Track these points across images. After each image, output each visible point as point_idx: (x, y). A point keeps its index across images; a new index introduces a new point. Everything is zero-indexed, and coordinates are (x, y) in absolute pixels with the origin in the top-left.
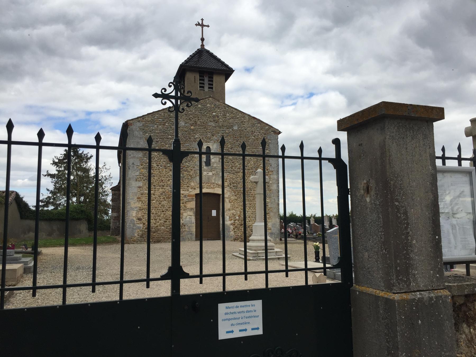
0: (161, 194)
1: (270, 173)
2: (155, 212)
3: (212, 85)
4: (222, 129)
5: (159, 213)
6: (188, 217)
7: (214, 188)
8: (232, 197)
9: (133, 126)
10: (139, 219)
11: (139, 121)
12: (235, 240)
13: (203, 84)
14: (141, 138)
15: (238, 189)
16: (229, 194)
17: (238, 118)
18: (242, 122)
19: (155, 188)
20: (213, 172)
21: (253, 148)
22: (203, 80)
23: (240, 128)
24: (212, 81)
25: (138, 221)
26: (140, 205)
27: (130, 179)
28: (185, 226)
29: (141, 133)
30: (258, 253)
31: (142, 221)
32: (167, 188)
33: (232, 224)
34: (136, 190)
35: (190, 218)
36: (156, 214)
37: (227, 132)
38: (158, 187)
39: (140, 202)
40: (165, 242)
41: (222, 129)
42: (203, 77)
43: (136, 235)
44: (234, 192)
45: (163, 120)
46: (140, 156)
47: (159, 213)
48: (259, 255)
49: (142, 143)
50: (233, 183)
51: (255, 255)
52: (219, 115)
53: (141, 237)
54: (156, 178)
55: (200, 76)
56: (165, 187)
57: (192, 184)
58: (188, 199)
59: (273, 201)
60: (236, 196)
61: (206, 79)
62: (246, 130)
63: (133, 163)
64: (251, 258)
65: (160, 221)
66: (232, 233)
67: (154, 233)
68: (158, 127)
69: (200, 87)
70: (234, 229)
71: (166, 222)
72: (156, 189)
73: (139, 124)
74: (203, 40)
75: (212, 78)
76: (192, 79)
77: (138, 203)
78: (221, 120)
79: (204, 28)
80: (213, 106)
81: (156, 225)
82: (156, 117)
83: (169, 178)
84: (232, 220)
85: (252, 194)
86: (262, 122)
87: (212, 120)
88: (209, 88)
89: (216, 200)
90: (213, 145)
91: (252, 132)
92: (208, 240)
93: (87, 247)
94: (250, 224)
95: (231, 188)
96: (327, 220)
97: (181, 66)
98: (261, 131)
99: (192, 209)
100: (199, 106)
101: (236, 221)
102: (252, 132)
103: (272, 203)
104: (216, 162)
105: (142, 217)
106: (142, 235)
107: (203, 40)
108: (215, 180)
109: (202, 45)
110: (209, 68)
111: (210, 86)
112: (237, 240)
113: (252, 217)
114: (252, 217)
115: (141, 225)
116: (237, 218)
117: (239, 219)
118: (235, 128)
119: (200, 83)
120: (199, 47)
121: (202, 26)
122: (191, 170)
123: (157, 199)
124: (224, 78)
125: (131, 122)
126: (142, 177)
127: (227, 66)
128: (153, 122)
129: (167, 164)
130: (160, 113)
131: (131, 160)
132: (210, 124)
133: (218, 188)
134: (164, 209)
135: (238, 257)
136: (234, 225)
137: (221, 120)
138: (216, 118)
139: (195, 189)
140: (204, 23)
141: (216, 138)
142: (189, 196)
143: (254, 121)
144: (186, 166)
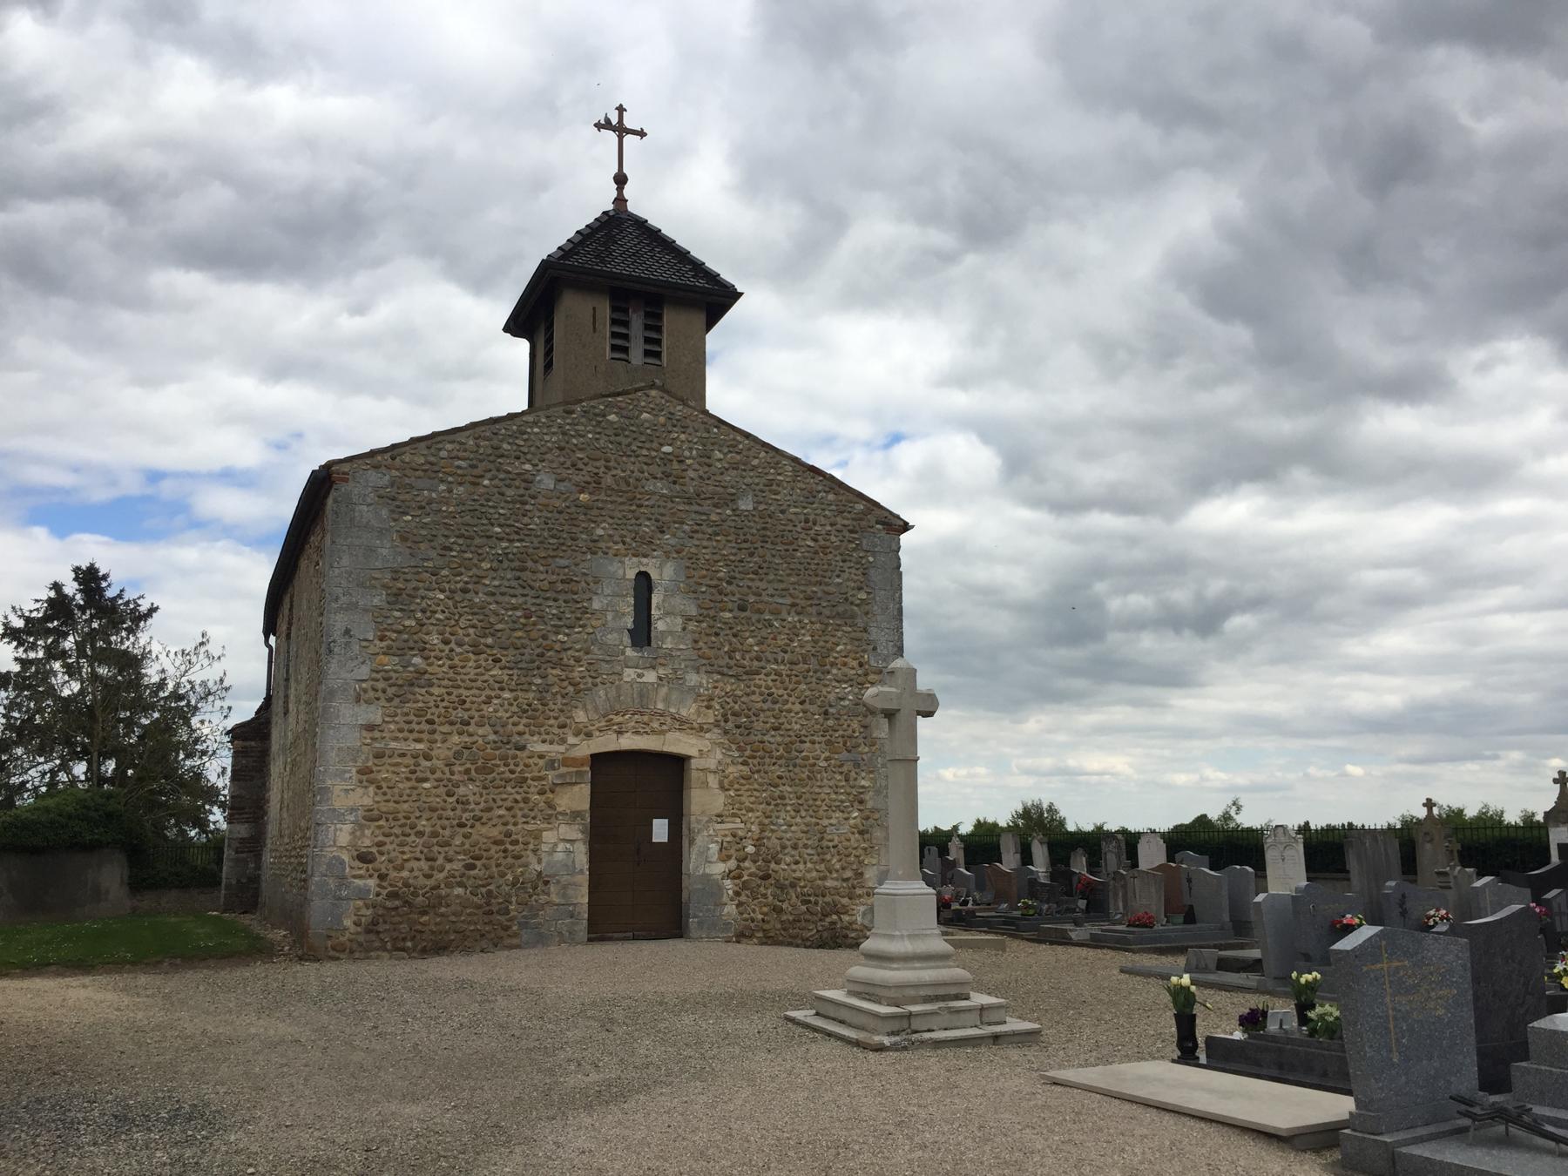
0: (457, 755)
1: (871, 677)
2: (428, 830)
3: (658, 342)
4: (696, 508)
5: (447, 833)
6: (561, 847)
7: (663, 733)
8: (731, 769)
9: (351, 484)
10: (364, 858)
11: (376, 467)
12: (741, 936)
13: (626, 337)
14: (381, 533)
15: (752, 737)
16: (719, 756)
17: (754, 468)
18: (770, 483)
19: (433, 732)
20: (661, 671)
21: (810, 583)
22: (626, 324)
23: (761, 507)
24: (659, 329)
25: (357, 864)
26: (367, 801)
27: (332, 694)
28: (546, 883)
29: (384, 513)
30: (910, 1015)
31: (376, 865)
32: (481, 731)
33: (728, 875)
34: (353, 739)
35: (568, 852)
36: (435, 834)
37: (714, 517)
38: (446, 728)
39: (372, 789)
40: (467, 951)
41: (696, 508)
42: (626, 311)
43: (348, 923)
44: (740, 749)
45: (473, 467)
46: (376, 601)
47: (447, 833)
48: (916, 1024)
49: (385, 552)
50: (735, 714)
51: (896, 1026)
52: (687, 453)
53: (368, 931)
55: (614, 309)
56: (471, 729)
57: (580, 716)
58: (561, 776)
60: (745, 763)
61: (637, 322)
62: (783, 512)
63: (347, 632)
64: (887, 1041)
65: (448, 866)
66: (730, 909)
67: (425, 913)
68: (450, 491)
69: (614, 348)
70: (737, 894)
71: (473, 867)
72: (437, 736)
73: (374, 477)
74: (621, 180)
75: (659, 317)
76: (580, 313)
77: (360, 791)
78: (691, 474)
79: (628, 139)
80: (662, 420)
82: (443, 454)
83: (488, 692)
84: (729, 857)
85: (806, 758)
86: (841, 484)
87: (658, 471)
88: (647, 353)
89: (663, 777)
90: (661, 567)
91: (807, 521)
93: (143, 979)
94: (798, 874)
95: (726, 732)
96: (1012, 850)
97: (546, 267)
98: (839, 519)
99: (576, 815)
100: (612, 417)
101: (747, 864)
102: (807, 521)
104: (671, 633)
105: (374, 850)
106: (374, 923)
107: (621, 180)
109: (620, 201)
110: (647, 281)
111: (649, 347)
112: (750, 937)
113: (806, 846)
114: (806, 846)
116: (750, 849)
118: (746, 504)
119: (614, 335)
120: (610, 207)
121: (621, 130)
122: (578, 660)
123: (438, 775)
124: (700, 318)
125: (346, 468)
126: (381, 685)
127: (713, 277)
128: (432, 471)
129: (485, 636)
130: (461, 437)
131: (339, 617)
132: (650, 486)
134: (466, 815)
135: (815, 1029)
137: (691, 474)
138: (676, 465)
139: (589, 735)
140: (628, 123)
141: (673, 541)
142: (567, 762)
143: (812, 481)
144: (557, 647)
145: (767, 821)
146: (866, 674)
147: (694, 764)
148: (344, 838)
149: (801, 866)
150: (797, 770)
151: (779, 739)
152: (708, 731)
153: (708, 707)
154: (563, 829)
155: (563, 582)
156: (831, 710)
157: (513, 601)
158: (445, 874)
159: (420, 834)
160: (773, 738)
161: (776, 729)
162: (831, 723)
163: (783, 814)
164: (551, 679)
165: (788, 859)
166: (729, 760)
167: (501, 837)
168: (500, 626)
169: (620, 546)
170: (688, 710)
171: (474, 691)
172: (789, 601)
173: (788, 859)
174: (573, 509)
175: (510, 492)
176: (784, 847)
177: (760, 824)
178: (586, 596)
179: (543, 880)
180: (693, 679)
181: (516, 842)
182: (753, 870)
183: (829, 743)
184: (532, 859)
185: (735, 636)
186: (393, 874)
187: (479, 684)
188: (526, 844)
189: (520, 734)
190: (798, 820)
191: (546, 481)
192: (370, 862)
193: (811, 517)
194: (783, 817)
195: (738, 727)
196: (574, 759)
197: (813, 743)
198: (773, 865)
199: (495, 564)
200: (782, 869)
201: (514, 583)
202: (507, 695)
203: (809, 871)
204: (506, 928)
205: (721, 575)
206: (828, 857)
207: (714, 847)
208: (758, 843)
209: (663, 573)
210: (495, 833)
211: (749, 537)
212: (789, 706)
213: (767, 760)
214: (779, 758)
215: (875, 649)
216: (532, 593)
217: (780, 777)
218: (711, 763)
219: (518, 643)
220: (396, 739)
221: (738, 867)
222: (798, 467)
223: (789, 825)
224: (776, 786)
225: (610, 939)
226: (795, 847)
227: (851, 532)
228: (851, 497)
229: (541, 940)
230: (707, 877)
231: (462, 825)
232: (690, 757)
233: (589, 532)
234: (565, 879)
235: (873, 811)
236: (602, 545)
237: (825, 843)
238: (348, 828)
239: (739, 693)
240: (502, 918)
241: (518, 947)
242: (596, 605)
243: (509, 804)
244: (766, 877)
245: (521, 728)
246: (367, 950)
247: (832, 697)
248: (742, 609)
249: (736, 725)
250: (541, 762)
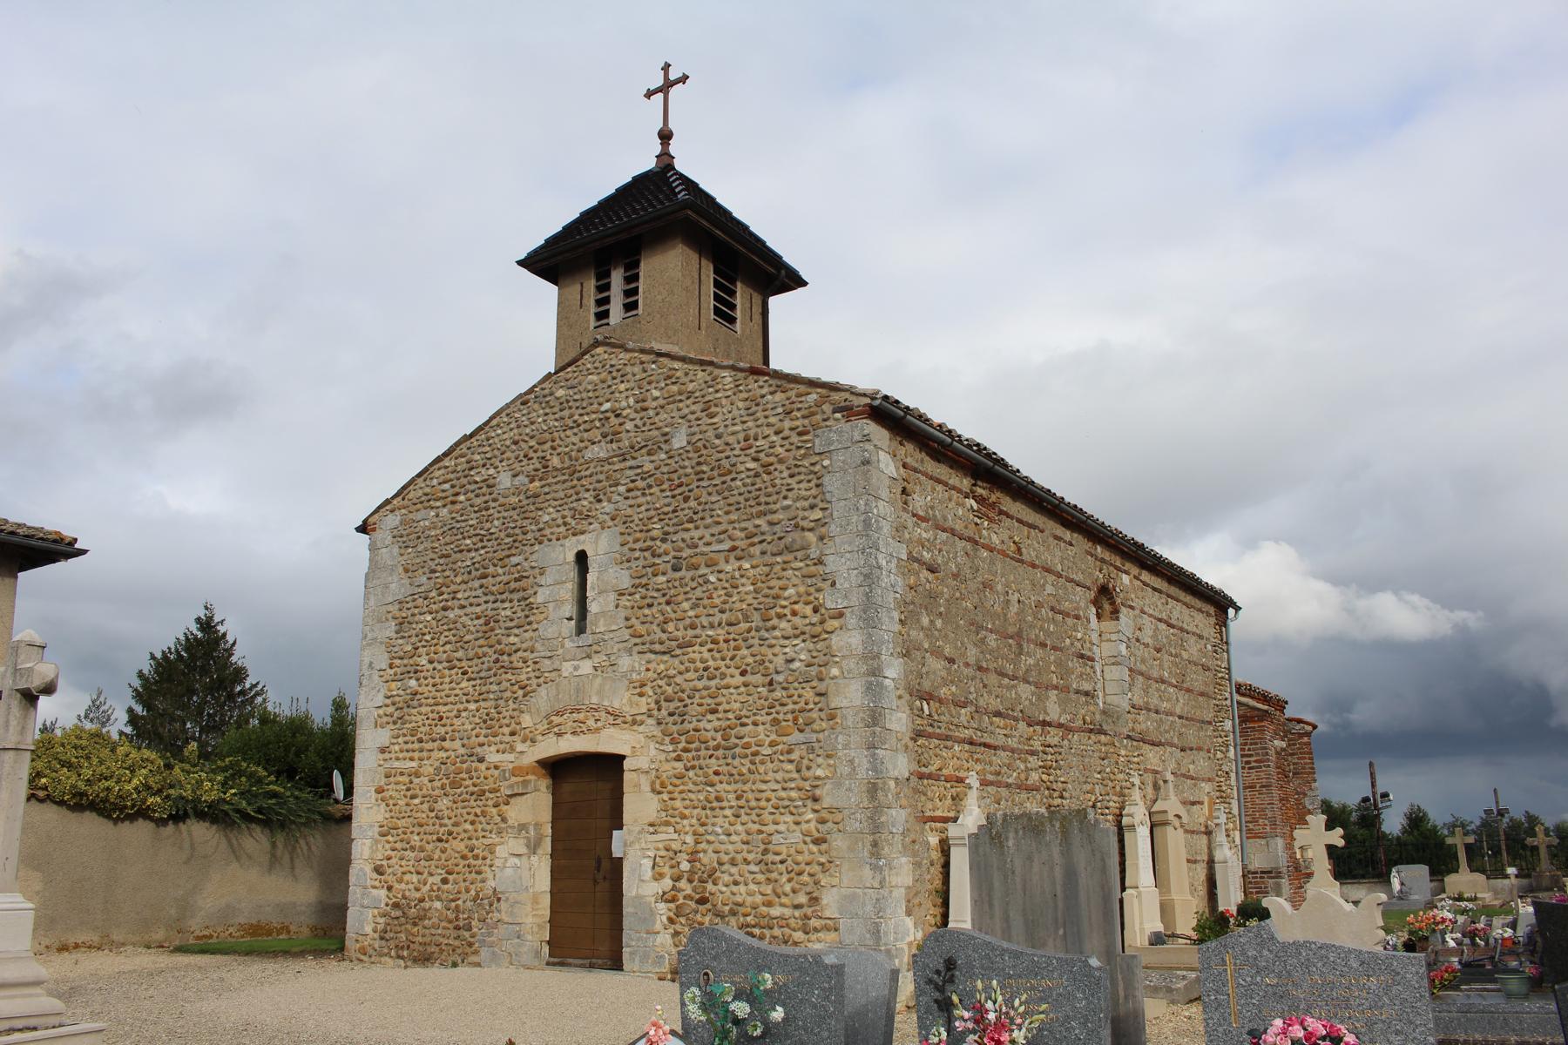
4: (628, 464)
7: (598, 730)
8: (667, 766)
14: (392, 569)
15: (687, 726)
16: (653, 752)
20: (596, 659)
25: (375, 876)
26: (380, 818)
29: (396, 550)
33: (665, 898)
37: (648, 467)
43: (368, 929)
44: (673, 742)
53: (382, 938)
54: (424, 709)
58: (511, 786)
59: (847, 770)
60: (678, 759)
65: (431, 880)
67: (415, 924)
73: (392, 520)
74: (665, 136)
81: (418, 895)
85: (747, 746)
87: (596, 435)
90: (596, 542)
92: (592, 966)
94: (739, 899)
98: (787, 424)
101: (683, 884)
103: (839, 785)
107: (665, 136)
108: (600, 692)
109: (665, 158)
115: (383, 892)
116: (685, 866)
117: (692, 872)
128: (427, 501)
132: (588, 455)
133: (612, 729)
136: (673, 900)
145: (701, 830)
146: (822, 622)
147: (627, 764)
148: (366, 854)
149: (742, 888)
150: (736, 762)
151: (717, 724)
152: (642, 723)
153: (641, 695)
154: (512, 842)
155: (516, 580)
156: (780, 678)
157: (478, 610)
158: (428, 887)
159: (413, 849)
160: (710, 724)
161: (714, 712)
162: (778, 694)
163: (720, 821)
164: (505, 684)
165: (726, 878)
166: (663, 757)
167: (466, 852)
168: (467, 638)
169: (562, 529)
170: (622, 700)
171: (450, 707)
172: (726, 546)
173: (726, 878)
174: (525, 502)
175: (478, 501)
176: (721, 864)
177: (695, 833)
178: (530, 592)
179: (497, 897)
180: (625, 662)
181: (476, 857)
182: (689, 891)
183: (776, 722)
184: (489, 875)
185: (668, 603)
186: (396, 886)
187: (452, 699)
188: (484, 858)
189: (481, 745)
190: (739, 828)
191: (505, 480)
192: (381, 874)
193: (752, 433)
194: (720, 824)
195: (671, 714)
196: (520, 768)
197: (755, 724)
198: (710, 886)
199: (466, 577)
200: (720, 891)
201: (479, 592)
202: (472, 706)
203: (750, 894)
204: (470, 945)
205: (655, 533)
206: (774, 875)
207: (648, 863)
208: (693, 857)
209: (600, 545)
210: (461, 847)
211: (683, 480)
212: (728, 680)
213: (703, 753)
214: (716, 748)
215: (833, 584)
216: (491, 598)
217: (716, 773)
218: (643, 763)
219: (480, 651)
220: (398, 759)
221: (674, 888)
222: (740, 375)
223: (728, 835)
224: (712, 785)
225: (569, 965)
226: (733, 863)
227: (800, 434)
228: (802, 388)
229: (495, 958)
230: (638, 897)
231: (440, 840)
232: (623, 757)
233: (536, 521)
234: (512, 896)
235: (830, 810)
236: (547, 532)
237: (770, 857)
238: (368, 842)
239: (672, 672)
240: (467, 934)
241: (478, 965)
242: (540, 599)
243: (471, 817)
244: (702, 901)
245: (482, 739)
246: (381, 955)
247: (780, 660)
248: (676, 569)
249: (672, 712)
250: (496, 773)
